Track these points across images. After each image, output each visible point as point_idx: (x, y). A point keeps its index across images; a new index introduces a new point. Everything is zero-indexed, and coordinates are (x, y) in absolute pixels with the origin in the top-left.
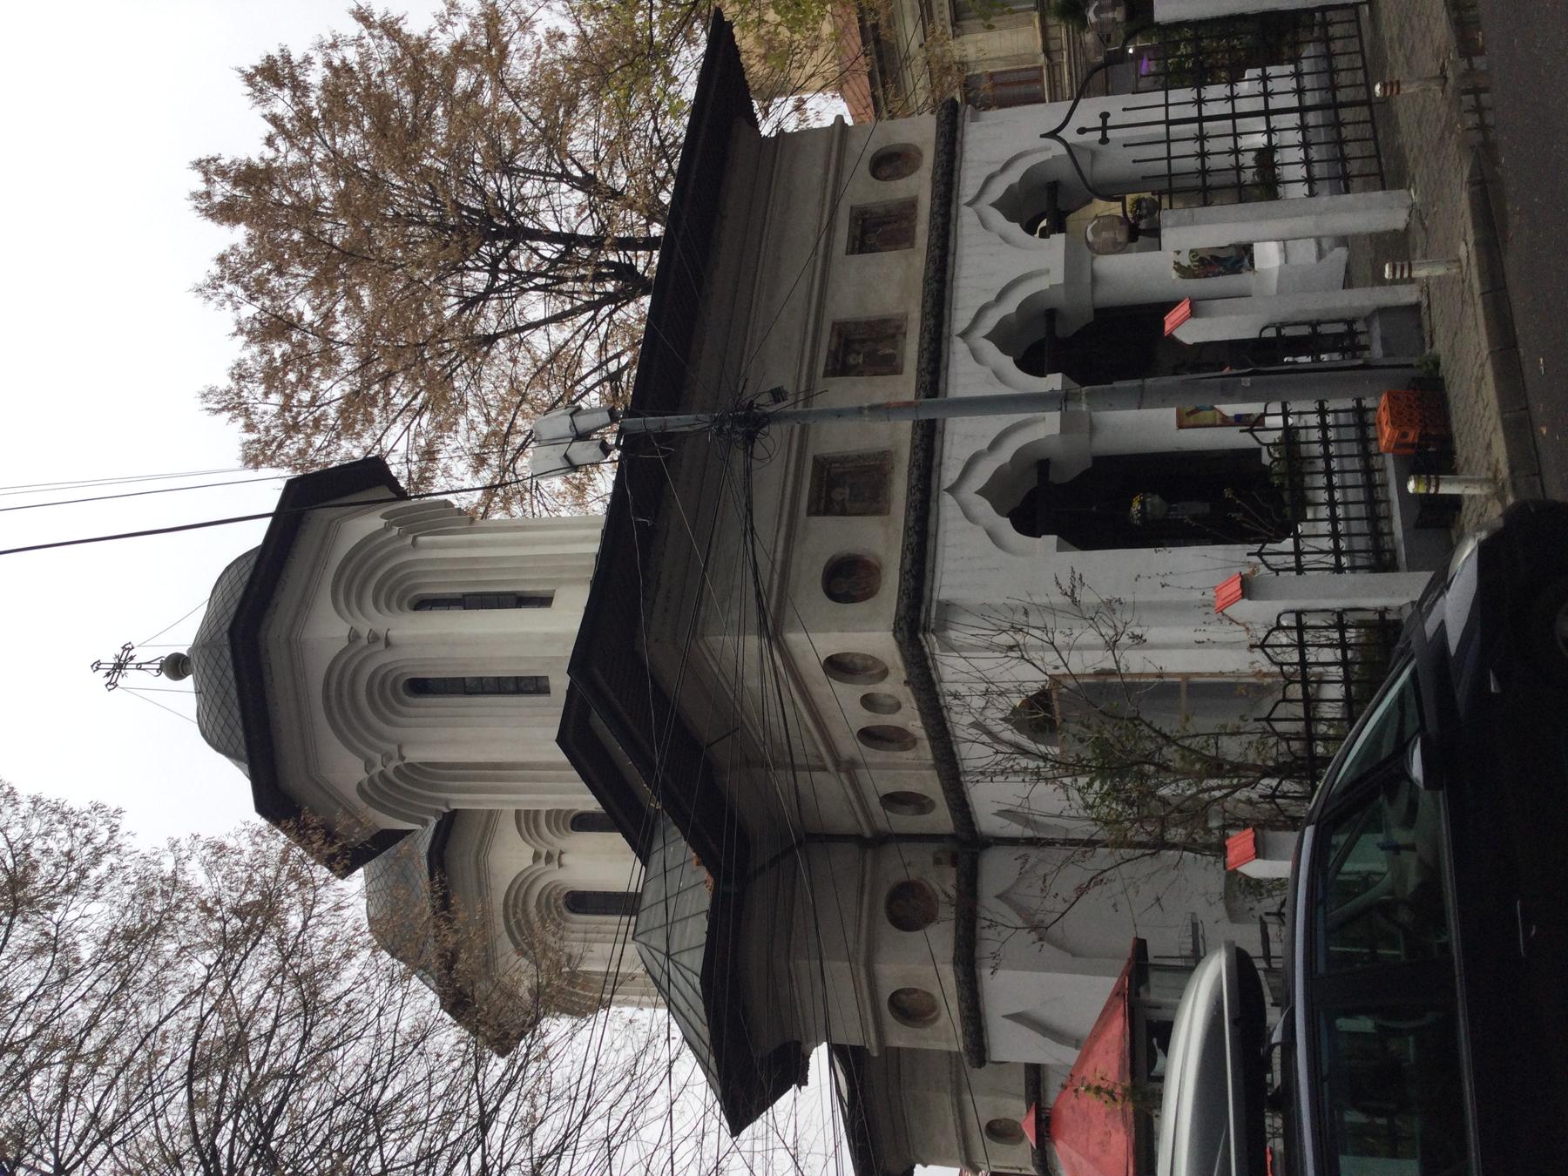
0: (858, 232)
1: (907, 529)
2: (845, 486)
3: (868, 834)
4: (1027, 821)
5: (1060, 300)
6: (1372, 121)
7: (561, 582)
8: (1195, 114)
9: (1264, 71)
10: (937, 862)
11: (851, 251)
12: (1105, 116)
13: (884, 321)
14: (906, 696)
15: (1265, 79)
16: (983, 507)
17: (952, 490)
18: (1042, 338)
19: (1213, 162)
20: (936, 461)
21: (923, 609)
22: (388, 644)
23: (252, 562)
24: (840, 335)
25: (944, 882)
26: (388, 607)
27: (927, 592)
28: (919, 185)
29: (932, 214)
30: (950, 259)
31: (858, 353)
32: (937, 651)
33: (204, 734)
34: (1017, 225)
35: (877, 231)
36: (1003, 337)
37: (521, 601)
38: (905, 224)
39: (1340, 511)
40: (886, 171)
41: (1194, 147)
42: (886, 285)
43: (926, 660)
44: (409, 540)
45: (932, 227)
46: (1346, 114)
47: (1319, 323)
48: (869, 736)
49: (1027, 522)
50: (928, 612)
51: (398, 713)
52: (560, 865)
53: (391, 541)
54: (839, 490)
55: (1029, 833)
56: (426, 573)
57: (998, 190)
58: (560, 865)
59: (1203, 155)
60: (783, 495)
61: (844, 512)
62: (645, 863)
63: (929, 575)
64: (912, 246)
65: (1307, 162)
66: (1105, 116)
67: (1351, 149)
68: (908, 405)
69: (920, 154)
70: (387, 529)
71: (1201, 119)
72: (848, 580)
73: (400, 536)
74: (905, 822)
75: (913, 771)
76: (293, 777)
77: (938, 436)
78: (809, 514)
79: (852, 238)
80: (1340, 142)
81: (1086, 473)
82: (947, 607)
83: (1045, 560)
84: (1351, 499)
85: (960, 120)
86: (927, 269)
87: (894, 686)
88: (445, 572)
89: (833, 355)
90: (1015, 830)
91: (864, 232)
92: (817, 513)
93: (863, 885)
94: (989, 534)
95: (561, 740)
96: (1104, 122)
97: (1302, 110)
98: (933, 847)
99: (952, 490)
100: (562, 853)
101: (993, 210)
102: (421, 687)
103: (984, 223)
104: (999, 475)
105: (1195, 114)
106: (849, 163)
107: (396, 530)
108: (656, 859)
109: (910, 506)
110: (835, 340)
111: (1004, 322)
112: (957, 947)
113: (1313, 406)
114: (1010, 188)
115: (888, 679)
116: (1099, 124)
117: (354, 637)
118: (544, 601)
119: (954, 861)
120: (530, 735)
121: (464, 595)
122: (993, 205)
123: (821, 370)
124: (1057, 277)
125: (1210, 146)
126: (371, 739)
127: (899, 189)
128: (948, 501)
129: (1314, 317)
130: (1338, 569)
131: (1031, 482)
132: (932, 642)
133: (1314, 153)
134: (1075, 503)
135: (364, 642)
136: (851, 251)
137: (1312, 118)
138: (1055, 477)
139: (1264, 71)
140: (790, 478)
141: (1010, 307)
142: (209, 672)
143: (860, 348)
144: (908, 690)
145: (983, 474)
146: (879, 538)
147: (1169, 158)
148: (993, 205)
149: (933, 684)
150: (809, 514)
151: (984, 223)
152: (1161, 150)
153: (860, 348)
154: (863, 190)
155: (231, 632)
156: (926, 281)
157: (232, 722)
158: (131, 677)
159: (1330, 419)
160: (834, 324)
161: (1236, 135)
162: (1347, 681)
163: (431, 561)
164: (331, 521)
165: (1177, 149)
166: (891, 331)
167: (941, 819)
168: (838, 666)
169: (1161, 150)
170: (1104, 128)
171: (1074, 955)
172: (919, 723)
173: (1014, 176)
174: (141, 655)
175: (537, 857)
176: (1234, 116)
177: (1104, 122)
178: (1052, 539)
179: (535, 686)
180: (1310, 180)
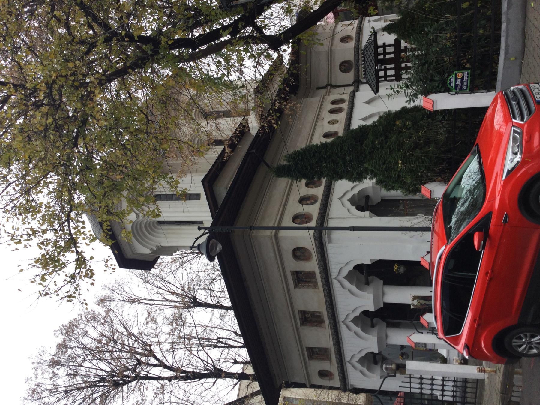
0: (296, 278)
6: (477, 388)
8: (420, 397)
19: (424, 391)
28: (312, 265)
35: (302, 279)
42: (320, 337)
67: (468, 390)
79: (294, 281)
85: (324, 242)
89: (301, 319)
94: (355, 333)
101: (345, 280)
103: (343, 286)
123: (299, 325)
151: (343, 286)
153: (309, 319)
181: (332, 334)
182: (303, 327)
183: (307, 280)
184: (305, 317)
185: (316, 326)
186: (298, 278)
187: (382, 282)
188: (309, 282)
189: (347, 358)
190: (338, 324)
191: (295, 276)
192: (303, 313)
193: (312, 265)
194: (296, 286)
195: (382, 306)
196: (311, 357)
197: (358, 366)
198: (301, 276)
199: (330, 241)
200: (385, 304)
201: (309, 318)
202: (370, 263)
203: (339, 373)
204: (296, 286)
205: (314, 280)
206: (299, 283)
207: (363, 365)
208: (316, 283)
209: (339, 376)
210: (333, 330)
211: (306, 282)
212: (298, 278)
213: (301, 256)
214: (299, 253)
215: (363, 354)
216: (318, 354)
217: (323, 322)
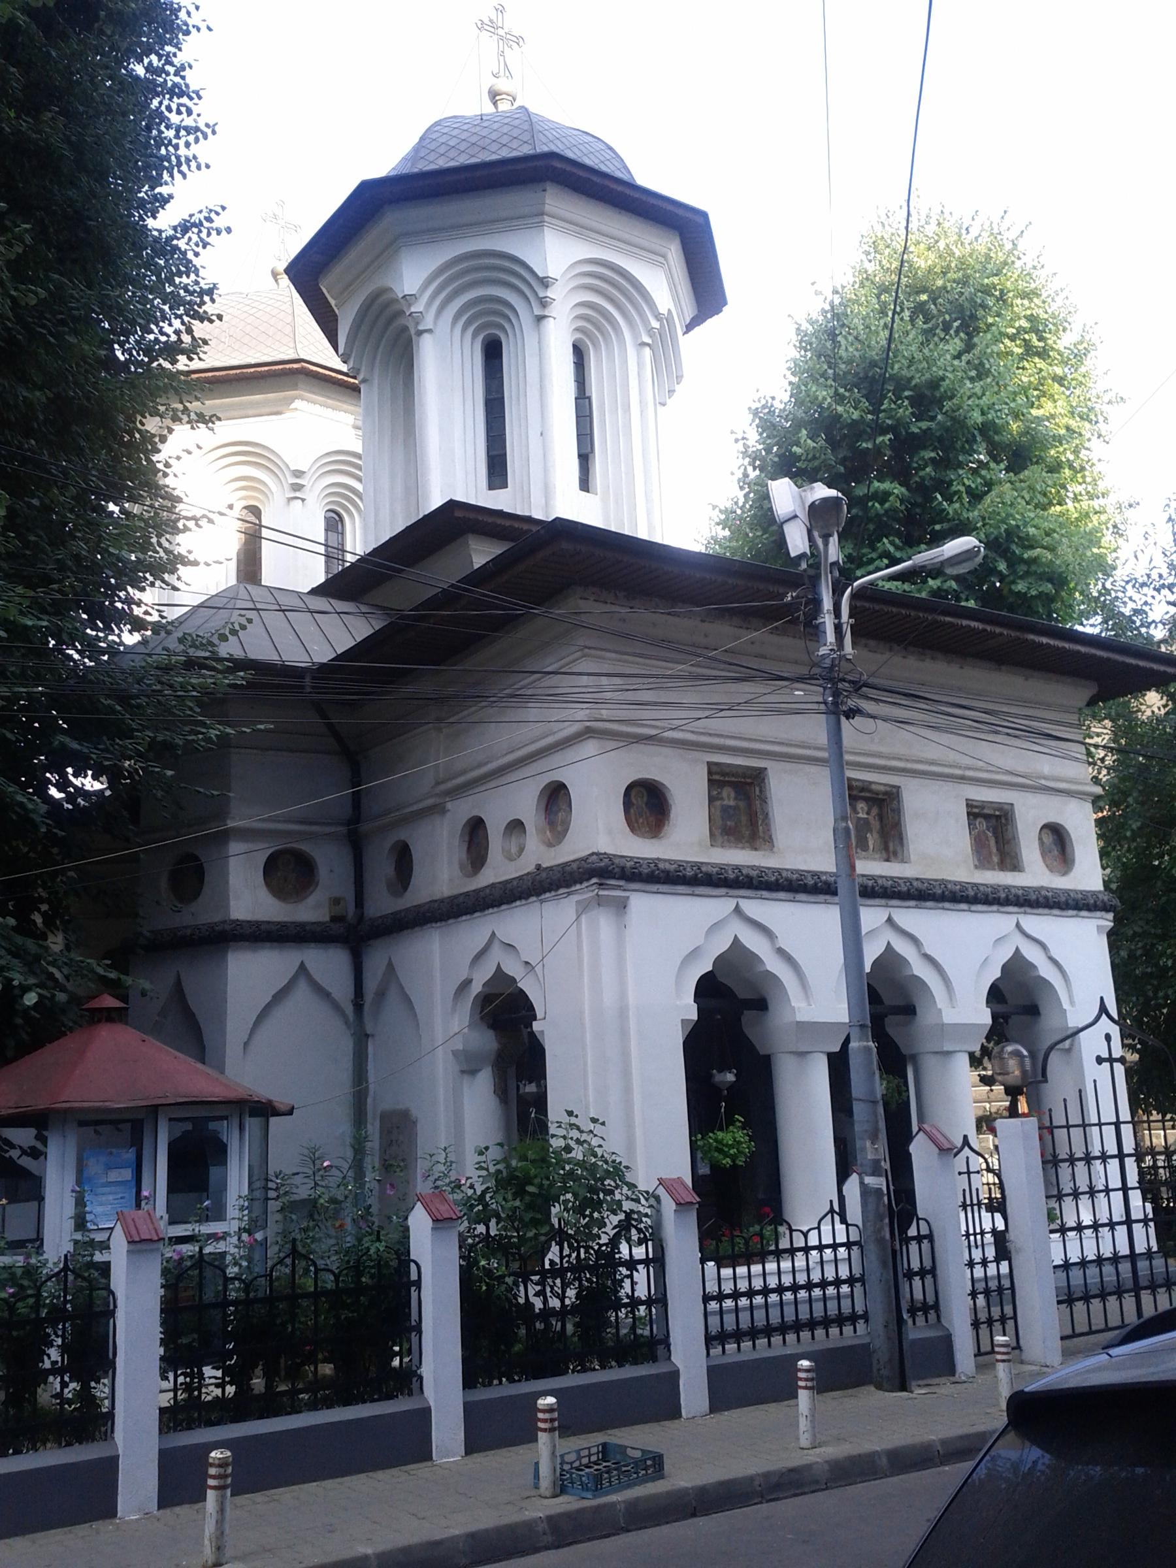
0: (986, 811)
1: (698, 865)
2: (740, 799)
3: (364, 827)
4: (381, 994)
5: (925, 1018)
7: (605, 501)
9: (1151, 1220)
10: (336, 901)
11: (970, 804)
12: (1100, 1060)
13: (901, 838)
14: (525, 866)
15: (1145, 1221)
16: (722, 945)
17: (737, 910)
20: (765, 894)
21: (621, 883)
22: (540, 319)
23: (618, 174)
24: (886, 793)
25: (310, 910)
26: (578, 317)
29: (1007, 888)
30: (964, 906)
31: (868, 813)
32: (575, 898)
33: (437, 124)
34: (998, 975)
37: (585, 459)
38: (996, 859)
39: (744, 1302)
40: (1048, 839)
43: (568, 886)
44: (647, 340)
45: (995, 888)
46: (1129, 1301)
47: (934, 1276)
48: (476, 829)
49: (708, 988)
51: (464, 329)
52: (290, 499)
53: (645, 322)
54: (733, 795)
55: (369, 996)
56: (611, 359)
57: (1032, 954)
58: (290, 499)
59: (1072, 1160)
61: (711, 799)
62: (314, 592)
63: (655, 887)
64: (976, 867)
65: (1083, 1263)
66: (1100, 1060)
68: (853, 868)
69: (1065, 873)
70: (658, 316)
71: (1121, 1156)
72: (647, 804)
73: (650, 331)
74: (381, 867)
75: (440, 873)
76: (392, 220)
78: (710, 765)
79: (983, 805)
80: (1103, 1296)
81: (751, 1048)
82: (622, 906)
83: (669, 1009)
84: (843, 1302)
85: (1098, 914)
86: (955, 883)
87: (537, 853)
88: (613, 377)
90: (371, 985)
91: (987, 817)
92: (710, 773)
93: (311, 823)
95: (451, 505)
96: (1105, 1060)
97: (1133, 1256)
98: (350, 896)
99: (737, 910)
100: (303, 500)
102: (493, 353)
104: (754, 958)
105: (1126, 1151)
106: (1056, 801)
107: (655, 324)
108: (320, 603)
109: (722, 868)
110: (882, 788)
111: (903, 961)
112: (257, 924)
113: (857, 1272)
114: (1033, 966)
115: (543, 848)
117: (545, 282)
118: (585, 484)
119: (334, 919)
120: (451, 473)
121: (589, 398)
122: (1017, 948)
124: (950, 1016)
126: (437, 303)
127: (1030, 849)
128: (730, 904)
129: (938, 1272)
130: (706, 1298)
131: (742, 994)
132: (585, 892)
133: (1092, 1271)
134: (728, 1033)
135: (541, 295)
136: (970, 804)
137: (1125, 1268)
138: (748, 1016)
139: (1151, 1220)
140: (745, 744)
141: (919, 969)
142: (505, 129)
143: (874, 813)
144: (531, 868)
145: (754, 942)
146: (688, 837)
147: (1068, 1127)
148: (1017, 948)
149: (538, 895)
150: (710, 765)
153: (874, 813)
154: (1031, 814)
155: (552, 155)
156: (943, 882)
157: (452, 154)
158: (489, 43)
159: (845, 1289)
162: (547, 1312)
163: (625, 362)
164: (664, 256)
165: (1077, 1133)
166: (891, 849)
167: (381, 904)
168: (556, 796)
169: (1075, 1119)
170: (1111, 1060)
171: (246, 1044)
172: (492, 880)
173: (1046, 971)
174: (513, 56)
175: (298, 474)
176: (1125, 1189)
177: (1105, 1060)
178: (694, 1016)
179: (497, 470)
180: (1066, 1266)
189: (758, 908)
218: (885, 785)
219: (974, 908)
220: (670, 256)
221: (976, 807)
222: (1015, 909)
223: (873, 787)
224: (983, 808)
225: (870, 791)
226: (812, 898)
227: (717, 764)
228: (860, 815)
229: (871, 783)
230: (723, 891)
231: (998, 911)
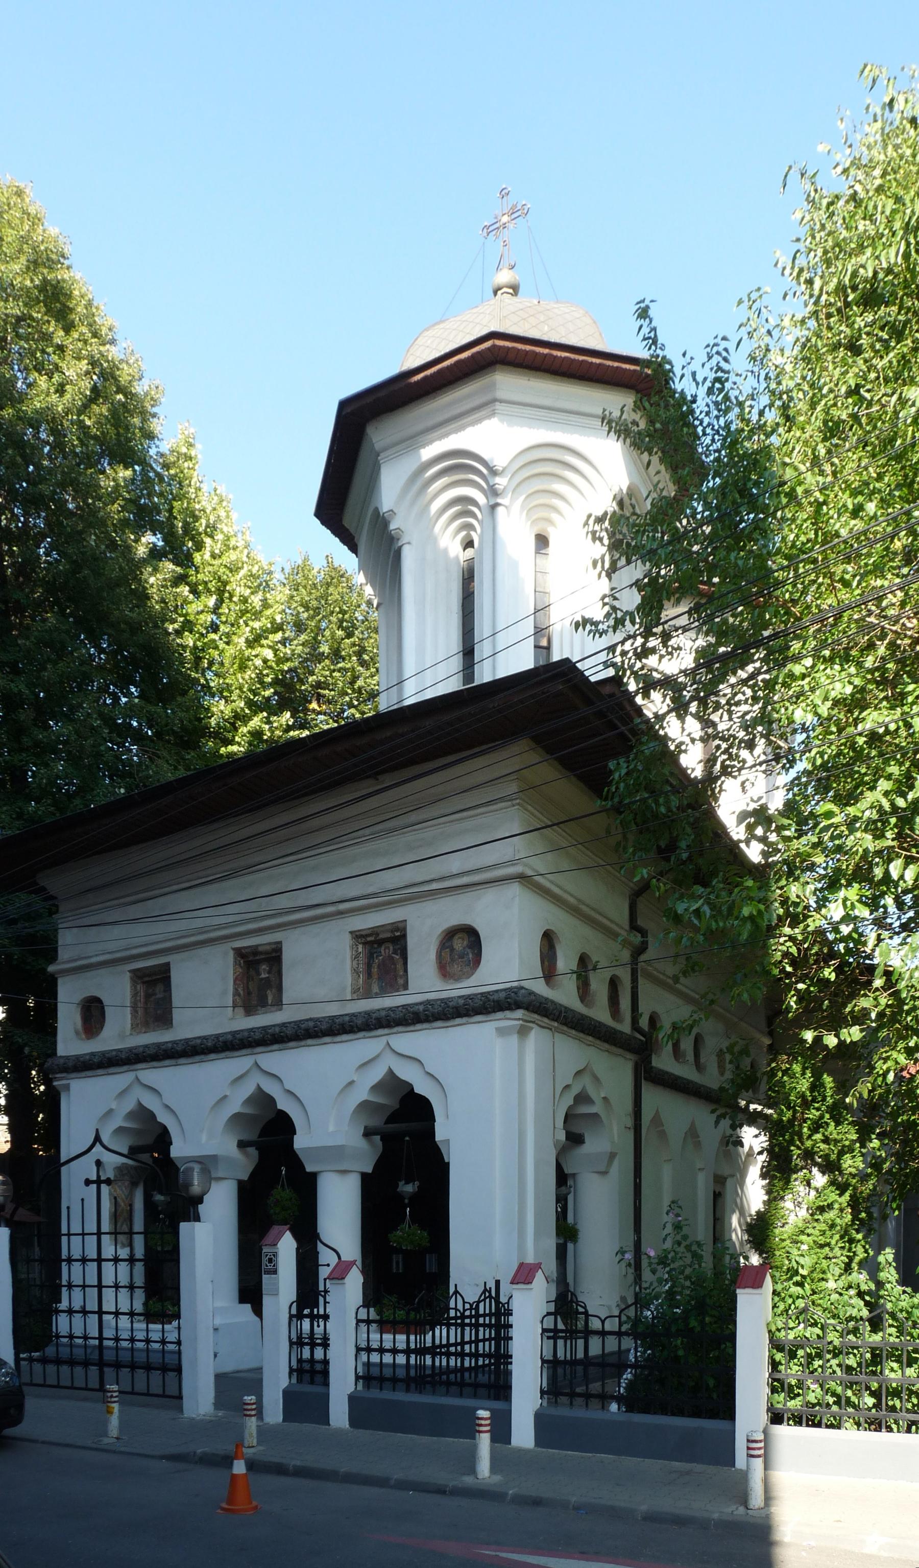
0: (382, 936)
18: (270, 1131)
27: (73, 1075)
31: (269, 972)
35: (383, 953)
36: (262, 1099)
40: (459, 944)
41: (76, 1254)
50: (62, 1079)
60: (76, 960)
77: (172, 1062)
79: (374, 931)
85: (500, 1015)
110: (268, 948)
116: (95, 1186)
123: (239, 944)
125: (77, 1266)
152: (76, 1228)
153: (260, 972)
160: (280, 943)
161: (117, 1286)
176: (100, 1287)
181: (217, 1036)
182: (231, 954)
183: (375, 970)
184: (259, 962)
185: (236, 993)
186: (381, 942)
187: (369, 1169)
188: (369, 975)
190: (249, 1051)
191: (389, 935)
192: (274, 956)
193: (424, 981)
194: (358, 936)
195: (309, 1169)
196: (139, 976)
197: (129, 1105)
198: (386, 951)
199: (501, 1032)
200: (314, 1177)
201: (259, 974)
202: (439, 1137)
203: (103, 1053)
204: (358, 936)
205: (375, 989)
206: (364, 944)
207: (131, 1115)
208: (368, 995)
209: (92, 1054)
210: (229, 1037)
211: (369, 966)
212: (381, 942)
213: (452, 949)
214: (462, 946)
215: (163, 1118)
216: (148, 996)
217: (249, 1010)
218: (269, 944)
219: (338, 1038)
220: (500, 394)
221: (367, 936)
222: (386, 1031)
223: (260, 949)
224: (378, 934)
225: (261, 953)
226: (190, 1060)
227: (138, 970)
228: (263, 976)
229: (257, 946)
230: (125, 1068)
231: (364, 1038)
